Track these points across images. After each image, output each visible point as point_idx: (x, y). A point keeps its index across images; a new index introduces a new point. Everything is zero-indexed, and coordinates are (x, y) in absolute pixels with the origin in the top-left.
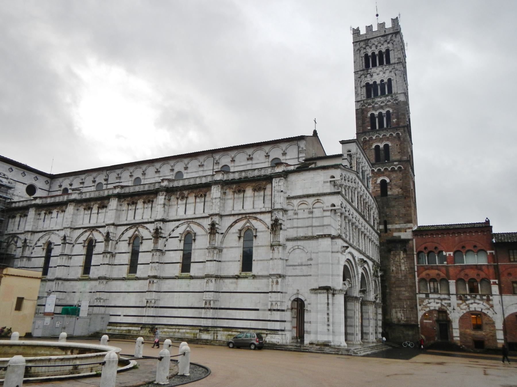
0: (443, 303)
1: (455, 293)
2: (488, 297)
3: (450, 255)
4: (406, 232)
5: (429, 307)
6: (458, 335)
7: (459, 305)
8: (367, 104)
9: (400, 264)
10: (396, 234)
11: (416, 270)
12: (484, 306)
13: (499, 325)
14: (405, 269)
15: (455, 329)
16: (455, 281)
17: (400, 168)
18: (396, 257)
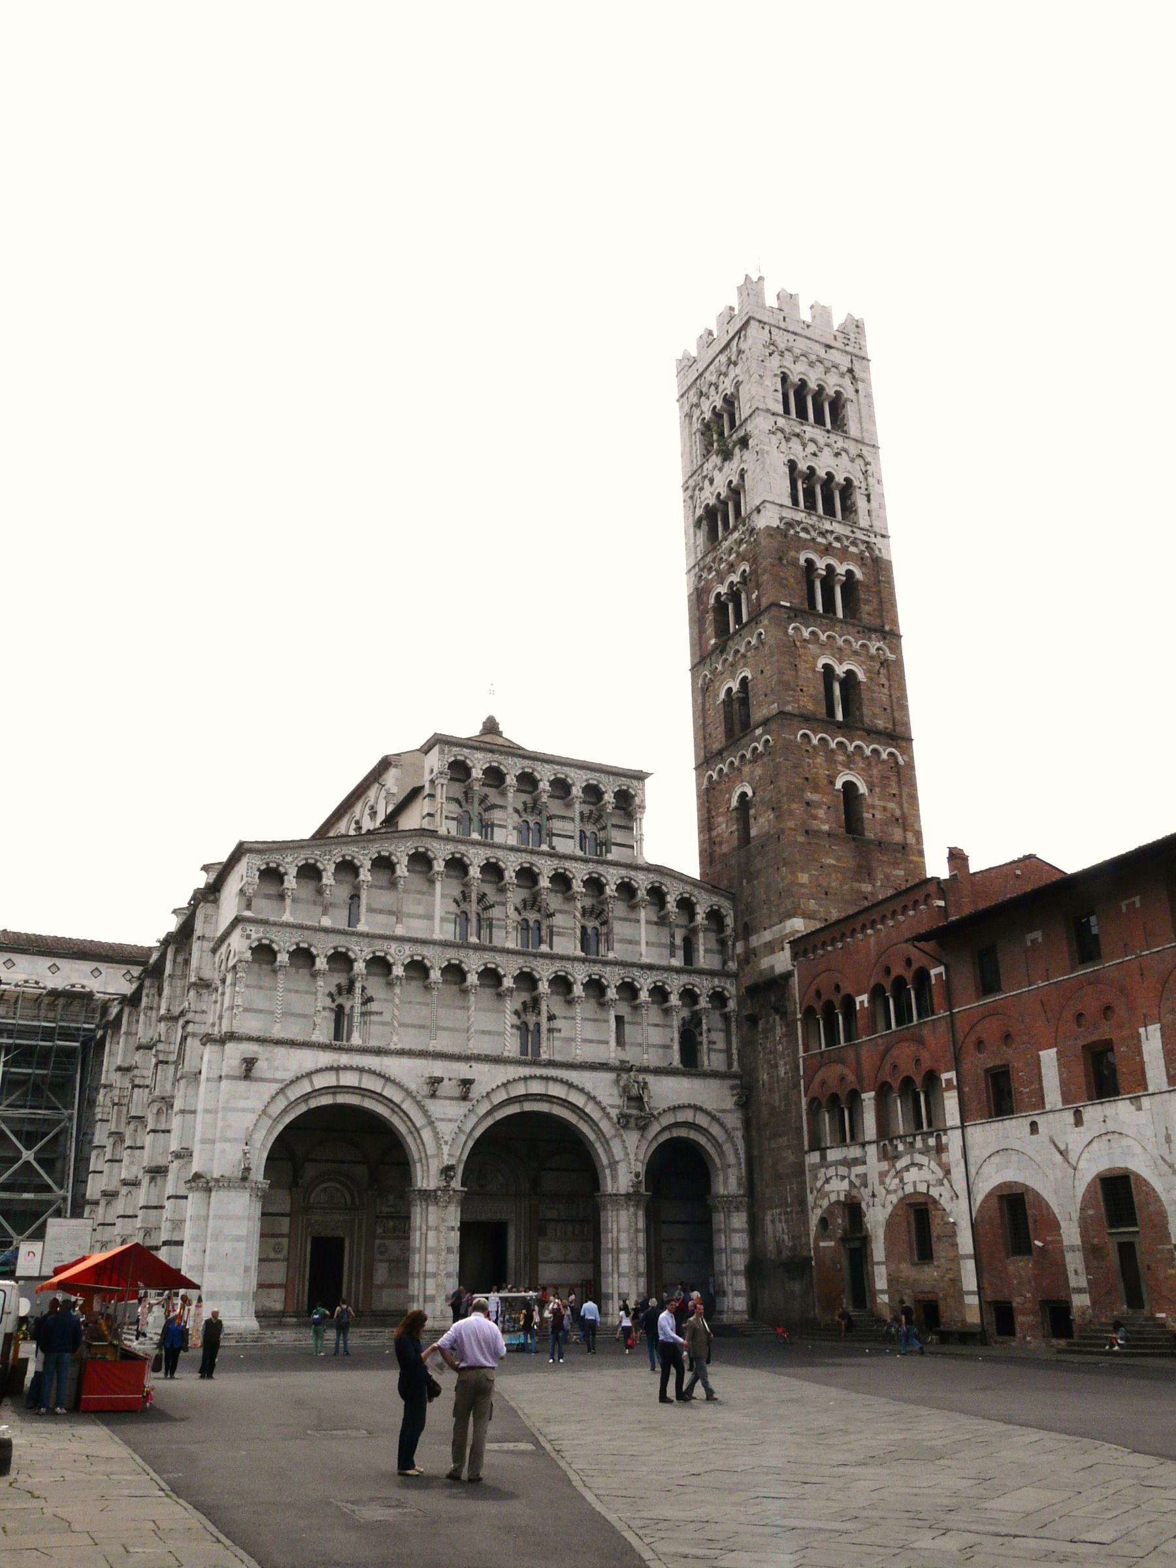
0: (853, 1178)
1: (874, 1138)
2: (938, 1137)
3: (862, 1003)
4: (783, 949)
5: (827, 1194)
6: (885, 1287)
7: (883, 1175)
8: (706, 570)
9: (775, 1059)
10: (765, 963)
11: (802, 1073)
12: (933, 1172)
13: (965, 1242)
14: (785, 1073)
15: (879, 1263)
16: (872, 1094)
17: (767, 741)
18: (767, 1038)
